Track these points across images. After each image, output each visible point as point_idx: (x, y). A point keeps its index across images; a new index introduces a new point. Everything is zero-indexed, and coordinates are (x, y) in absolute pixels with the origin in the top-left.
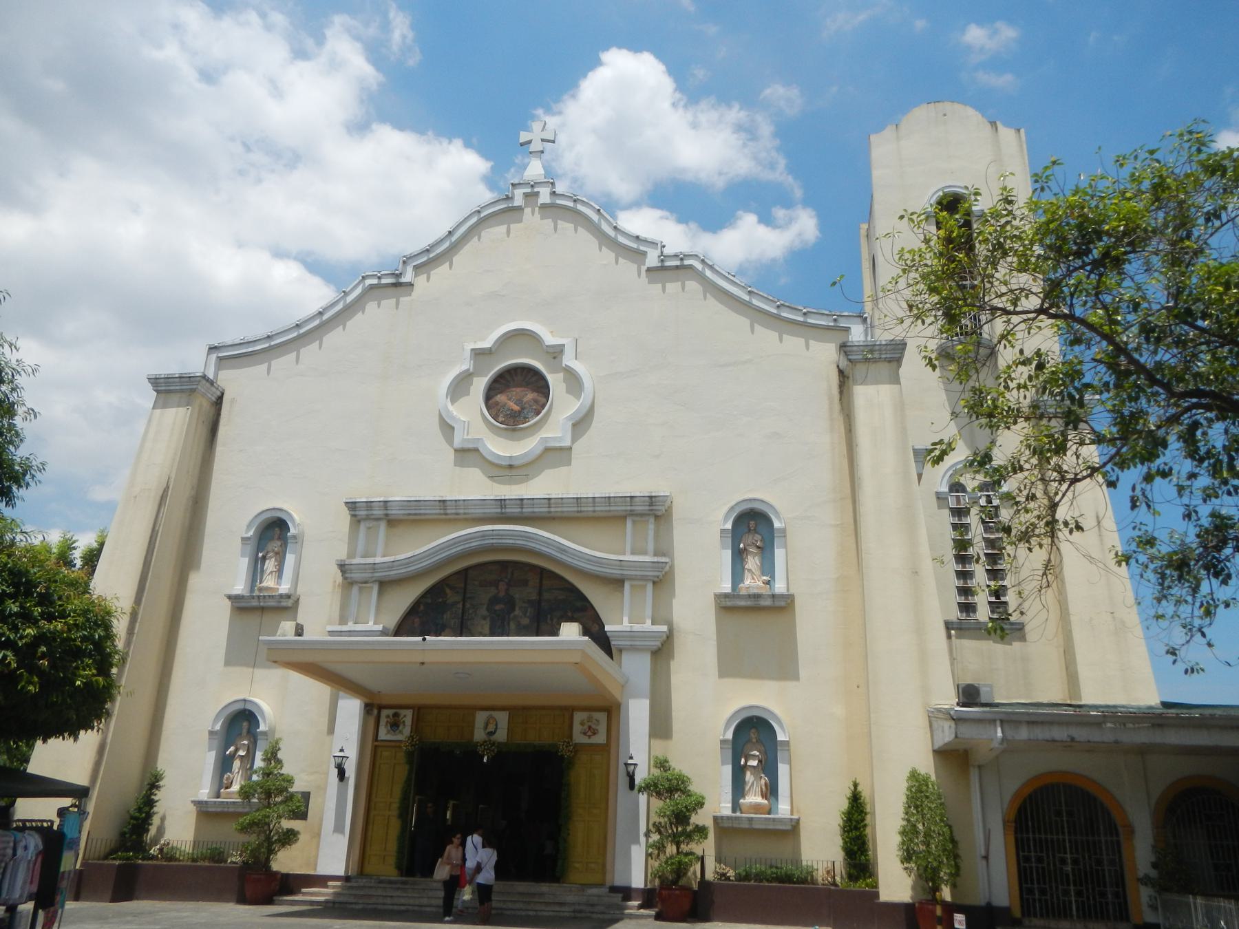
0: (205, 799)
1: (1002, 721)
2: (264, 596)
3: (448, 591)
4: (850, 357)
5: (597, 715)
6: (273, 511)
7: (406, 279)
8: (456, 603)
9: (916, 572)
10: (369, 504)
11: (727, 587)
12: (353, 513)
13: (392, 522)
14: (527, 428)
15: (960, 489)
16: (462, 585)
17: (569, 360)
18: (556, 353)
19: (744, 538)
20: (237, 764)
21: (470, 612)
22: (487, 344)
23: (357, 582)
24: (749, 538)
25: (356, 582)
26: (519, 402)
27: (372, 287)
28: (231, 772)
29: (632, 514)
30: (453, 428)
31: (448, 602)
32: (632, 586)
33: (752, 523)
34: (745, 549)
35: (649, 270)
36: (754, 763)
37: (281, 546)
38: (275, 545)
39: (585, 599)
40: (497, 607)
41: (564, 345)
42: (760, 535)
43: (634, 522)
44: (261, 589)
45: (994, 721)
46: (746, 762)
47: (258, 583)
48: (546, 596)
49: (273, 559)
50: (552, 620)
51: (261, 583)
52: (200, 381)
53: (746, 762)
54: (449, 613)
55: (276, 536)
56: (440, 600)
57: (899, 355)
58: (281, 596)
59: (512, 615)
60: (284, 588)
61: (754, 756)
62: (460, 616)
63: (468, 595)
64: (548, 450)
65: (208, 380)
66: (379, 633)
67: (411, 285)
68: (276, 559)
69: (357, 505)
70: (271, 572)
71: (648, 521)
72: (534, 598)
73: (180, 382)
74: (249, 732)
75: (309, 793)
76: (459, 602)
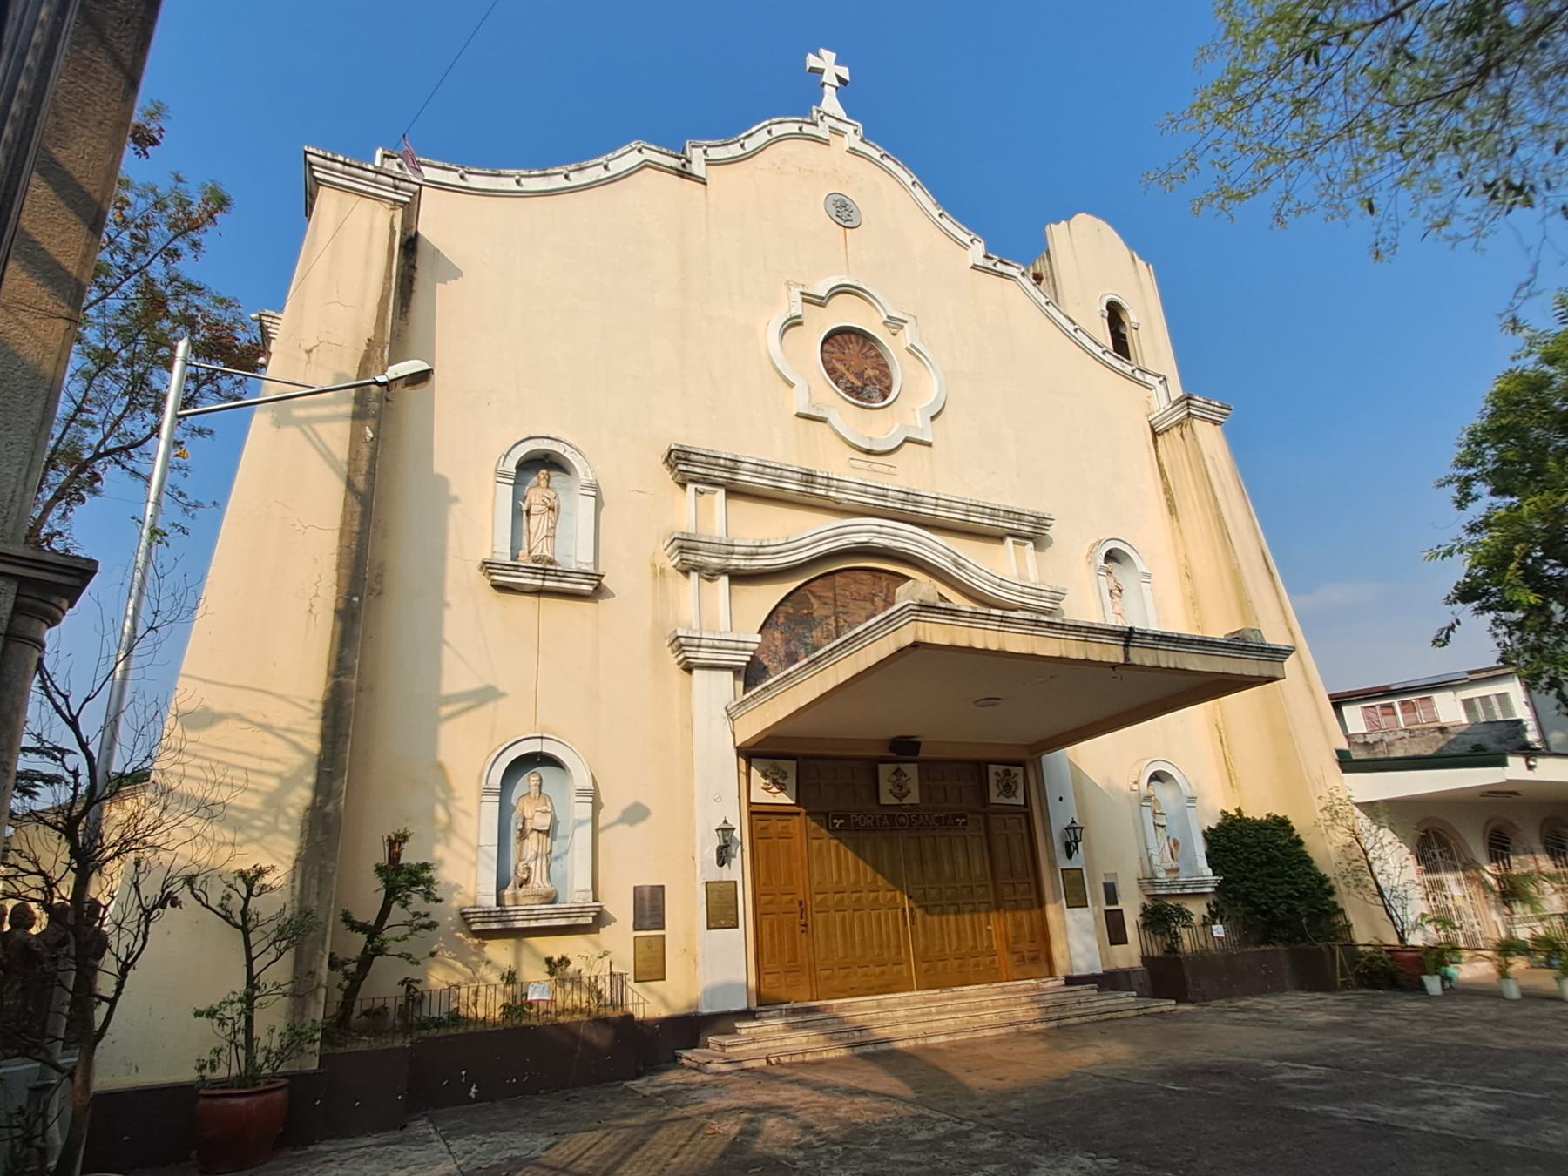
3: (813, 600)
4: (1192, 411)
5: (1014, 769)
8: (828, 617)
10: (710, 459)
26: (859, 375)
31: (815, 614)
41: (906, 322)
43: (1014, 543)
52: (414, 193)
54: (819, 629)
56: (805, 611)
76: (828, 617)
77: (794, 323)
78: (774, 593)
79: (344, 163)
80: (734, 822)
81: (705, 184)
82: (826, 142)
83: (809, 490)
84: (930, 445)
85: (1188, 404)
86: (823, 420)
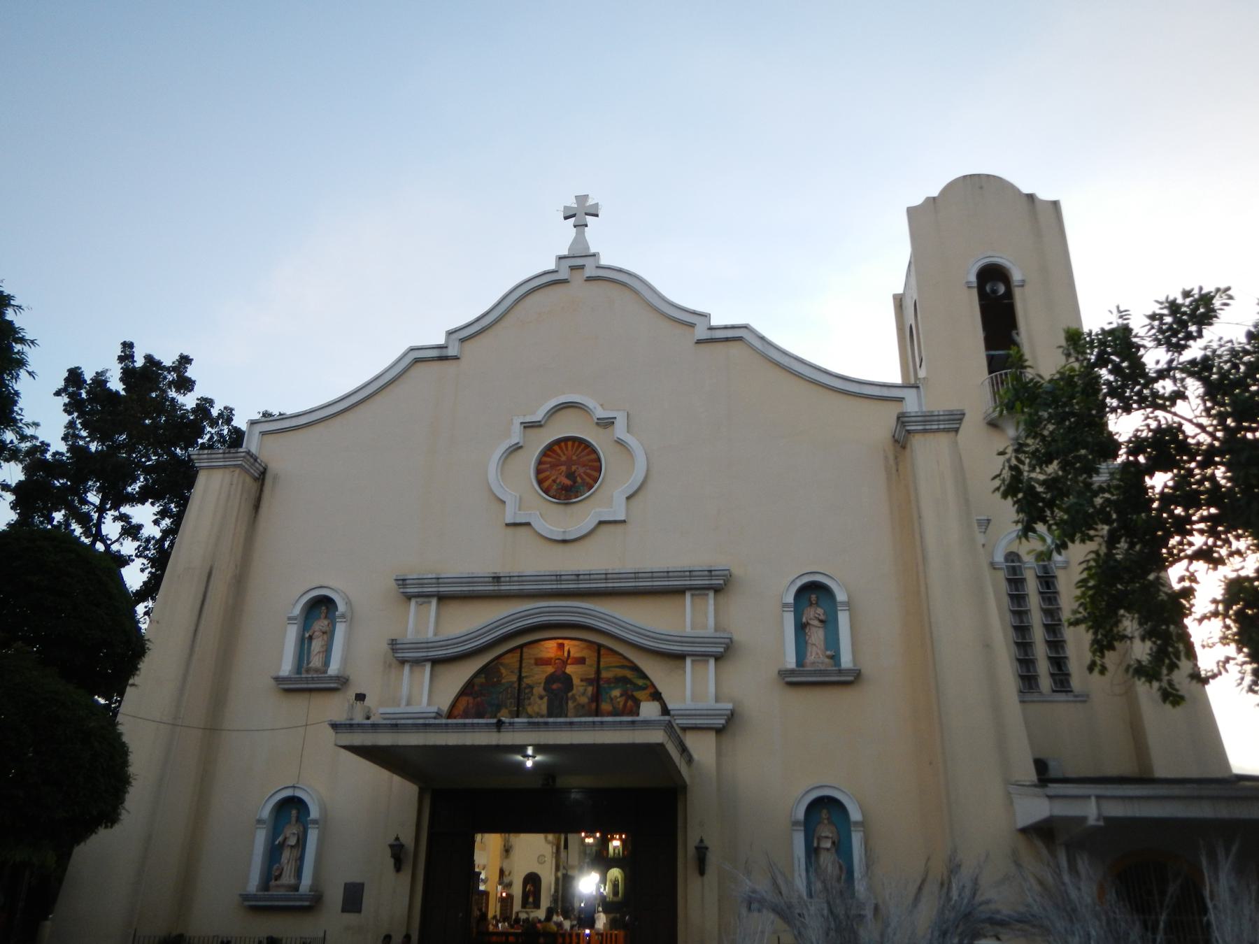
0: (255, 893)
1: (1098, 797)
2: (313, 678)
4: (908, 428)
6: (320, 589)
7: (451, 352)
9: (988, 646)
10: (420, 582)
11: (791, 662)
12: (402, 590)
13: (442, 598)
14: (580, 501)
15: (1015, 558)
16: (517, 665)
17: (620, 430)
18: (607, 423)
19: (805, 612)
20: (286, 854)
21: (527, 691)
22: (538, 416)
23: (407, 661)
25: (407, 661)
27: (417, 361)
28: (279, 862)
29: (691, 588)
30: (504, 502)
31: (503, 681)
32: (693, 661)
33: (813, 597)
34: (808, 624)
35: (699, 342)
36: (828, 844)
37: (328, 625)
38: (321, 624)
39: (645, 677)
40: (555, 686)
41: (615, 418)
42: (822, 608)
43: (692, 595)
44: (308, 671)
45: (1089, 797)
46: (818, 844)
47: (305, 665)
48: (605, 674)
49: (320, 639)
51: (308, 664)
52: (244, 457)
53: (818, 844)
55: (323, 615)
57: (957, 426)
58: (331, 677)
59: (570, 694)
60: (334, 669)
61: (827, 837)
62: (516, 695)
63: (523, 675)
64: (601, 523)
65: (251, 456)
66: (434, 715)
67: (456, 358)
68: (323, 639)
69: (408, 582)
70: (319, 652)
71: (707, 595)
72: (592, 676)
73: (224, 458)
74: (298, 820)
75: (362, 885)
77: (517, 448)
78: (460, 676)
79: (208, 454)
80: (408, 839)
81: (458, 358)
82: (565, 281)
83: (496, 588)
84: (624, 522)
85: (903, 422)
86: (528, 524)
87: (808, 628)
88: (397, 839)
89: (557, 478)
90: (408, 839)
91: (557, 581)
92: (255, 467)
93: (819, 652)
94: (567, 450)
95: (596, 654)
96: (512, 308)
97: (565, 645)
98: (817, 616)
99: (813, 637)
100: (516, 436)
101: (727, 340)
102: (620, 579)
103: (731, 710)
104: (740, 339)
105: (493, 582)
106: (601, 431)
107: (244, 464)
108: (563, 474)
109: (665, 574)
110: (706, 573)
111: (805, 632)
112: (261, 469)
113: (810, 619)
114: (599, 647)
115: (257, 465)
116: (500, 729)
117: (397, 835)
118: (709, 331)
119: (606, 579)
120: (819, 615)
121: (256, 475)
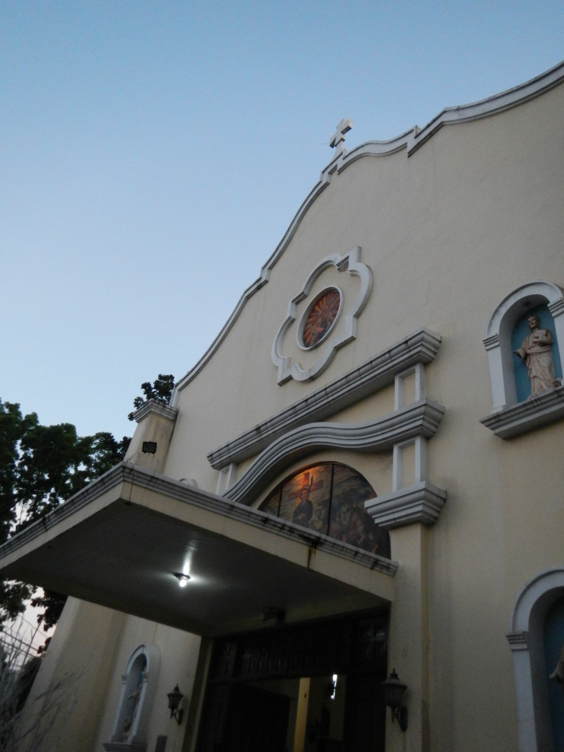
18: (344, 265)
24: (531, 339)
27: (248, 298)
35: (410, 154)
42: (544, 329)
48: (336, 492)
50: (340, 517)
52: (151, 405)
64: (338, 348)
67: (266, 282)
82: (327, 184)
83: (259, 438)
84: (352, 339)
86: (290, 378)
87: (528, 359)
88: (177, 689)
89: (315, 330)
90: (187, 690)
91: (294, 413)
92: (167, 412)
93: (543, 383)
94: (323, 304)
95: (330, 475)
96: (298, 227)
97: (310, 474)
98: (536, 340)
99: (533, 370)
100: (288, 311)
101: (431, 134)
102: (336, 389)
103: (424, 489)
104: (441, 125)
105: (257, 434)
106: (343, 273)
107: (153, 410)
108: (319, 325)
109: (369, 366)
110: (403, 346)
111: (526, 365)
112: (174, 413)
113: (529, 349)
114: (334, 464)
115: (168, 410)
116: (46, 527)
117: (177, 685)
118: (417, 139)
119: (327, 394)
120: (538, 338)
121: (171, 418)
